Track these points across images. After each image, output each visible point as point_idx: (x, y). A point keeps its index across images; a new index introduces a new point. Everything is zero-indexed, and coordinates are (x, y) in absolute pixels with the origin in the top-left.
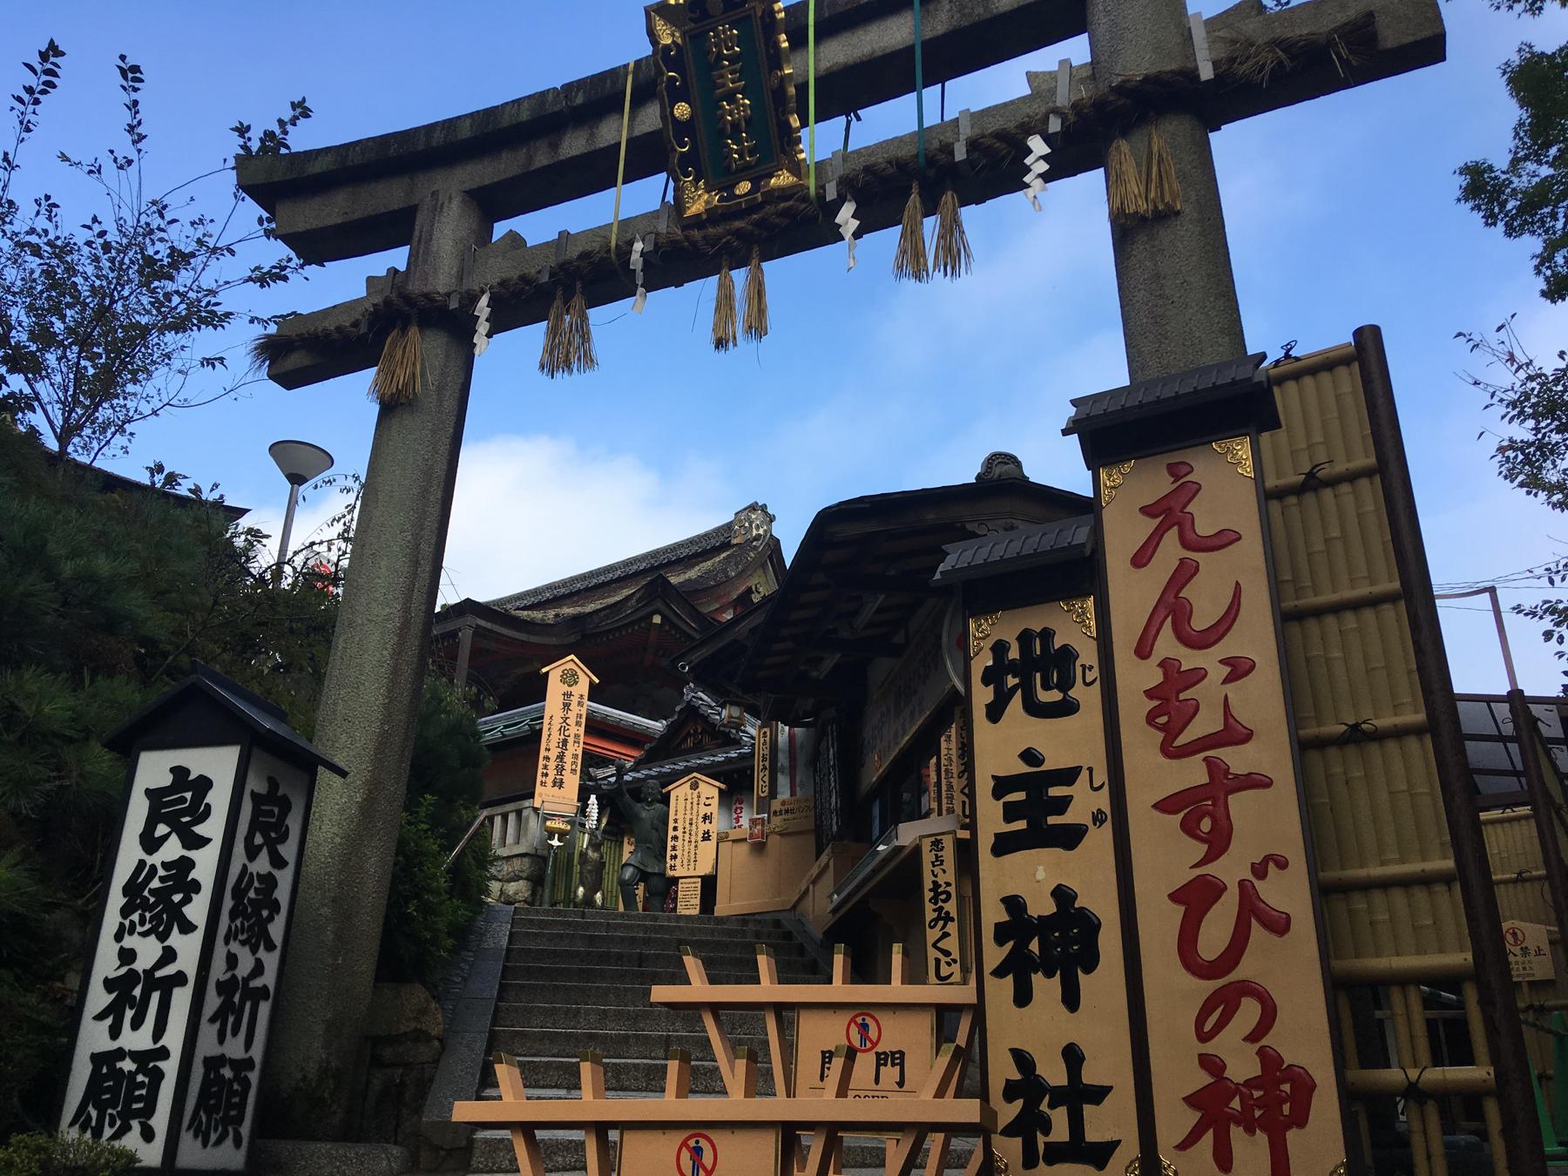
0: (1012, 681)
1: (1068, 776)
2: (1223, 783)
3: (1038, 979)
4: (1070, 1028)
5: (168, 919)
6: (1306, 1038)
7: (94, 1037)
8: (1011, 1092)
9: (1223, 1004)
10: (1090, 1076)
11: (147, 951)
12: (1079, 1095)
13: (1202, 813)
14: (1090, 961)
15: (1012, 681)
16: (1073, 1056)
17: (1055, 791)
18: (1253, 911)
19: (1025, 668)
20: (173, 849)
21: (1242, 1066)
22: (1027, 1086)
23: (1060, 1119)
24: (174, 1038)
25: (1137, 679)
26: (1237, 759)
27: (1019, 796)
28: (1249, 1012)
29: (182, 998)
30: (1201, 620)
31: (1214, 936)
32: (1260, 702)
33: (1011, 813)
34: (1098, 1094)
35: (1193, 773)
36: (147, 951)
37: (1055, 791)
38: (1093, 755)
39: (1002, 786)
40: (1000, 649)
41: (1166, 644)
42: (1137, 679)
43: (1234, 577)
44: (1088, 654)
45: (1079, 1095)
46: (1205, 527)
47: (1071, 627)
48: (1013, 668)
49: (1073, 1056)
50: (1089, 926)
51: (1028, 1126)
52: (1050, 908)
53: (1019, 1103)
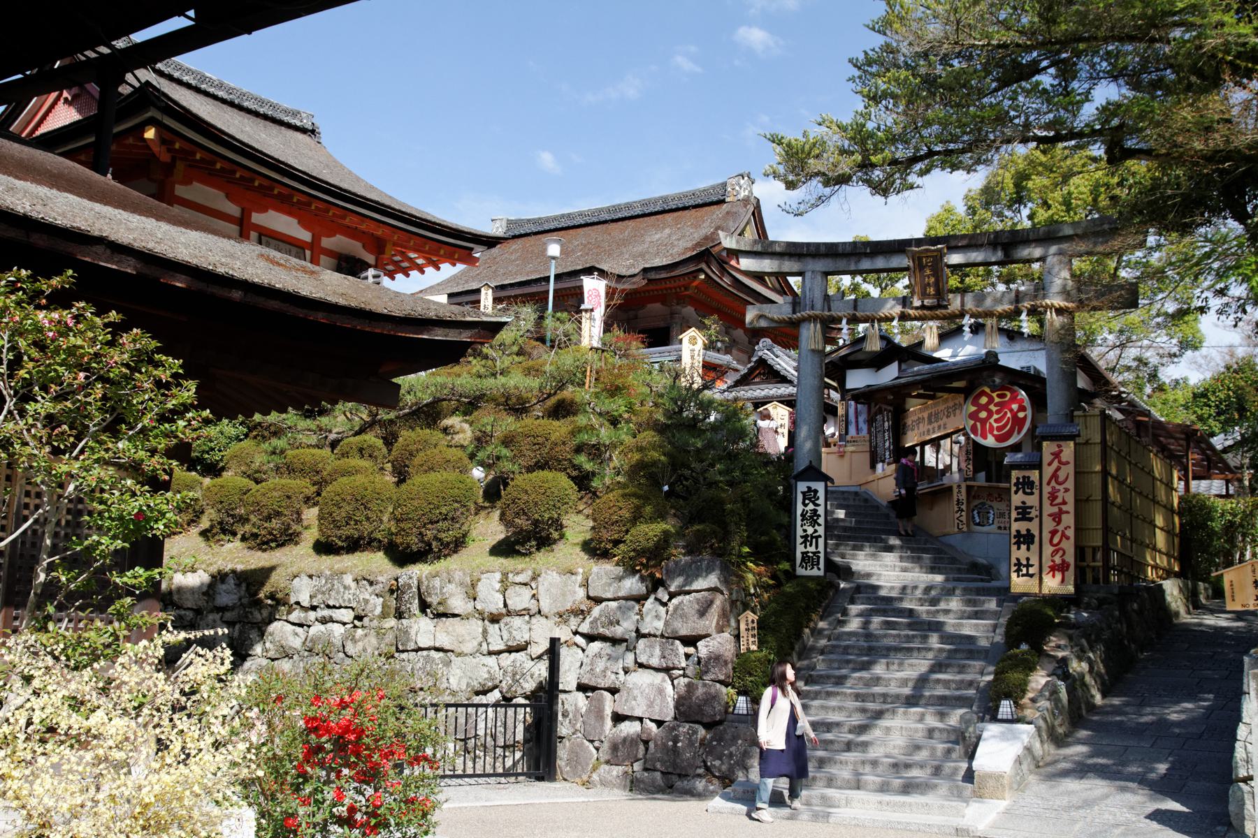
1: (1031, 507)
2: (1061, 512)
4: (1027, 554)
5: (814, 523)
6: (1070, 558)
7: (800, 549)
9: (1056, 552)
11: (810, 530)
12: (1028, 566)
13: (1057, 518)
14: (1033, 542)
16: (1028, 559)
18: (1063, 535)
19: (1023, 484)
20: (811, 506)
21: (1058, 560)
22: (1019, 564)
24: (821, 548)
25: (1047, 490)
26: (1064, 508)
28: (1061, 553)
29: (821, 541)
30: (1061, 479)
31: (1056, 541)
32: (1070, 498)
35: (1055, 509)
36: (810, 530)
38: (1037, 504)
39: (1017, 508)
40: (1018, 479)
41: (1053, 484)
42: (1047, 490)
43: (1069, 470)
44: (1037, 483)
46: (1064, 460)
47: (1034, 475)
49: (1028, 559)
50: (1033, 536)
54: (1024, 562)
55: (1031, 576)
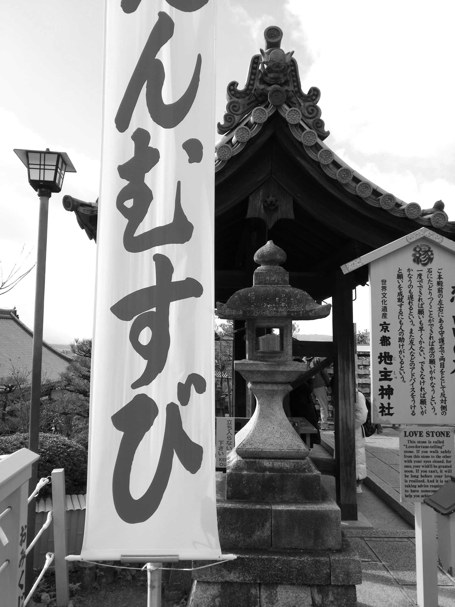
0: (383, 359)
1: (391, 372)
3: (385, 396)
8: (380, 408)
10: (391, 406)
12: (389, 408)
15: (383, 359)
16: (389, 404)
17: (388, 374)
23: (387, 411)
27: (383, 374)
33: (382, 376)
34: (392, 408)
37: (388, 374)
45: (389, 408)
48: (383, 357)
49: (389, 404)
51: (382, 412)
52: (387, 387)
54: (386, 406)
55: (391, 415)
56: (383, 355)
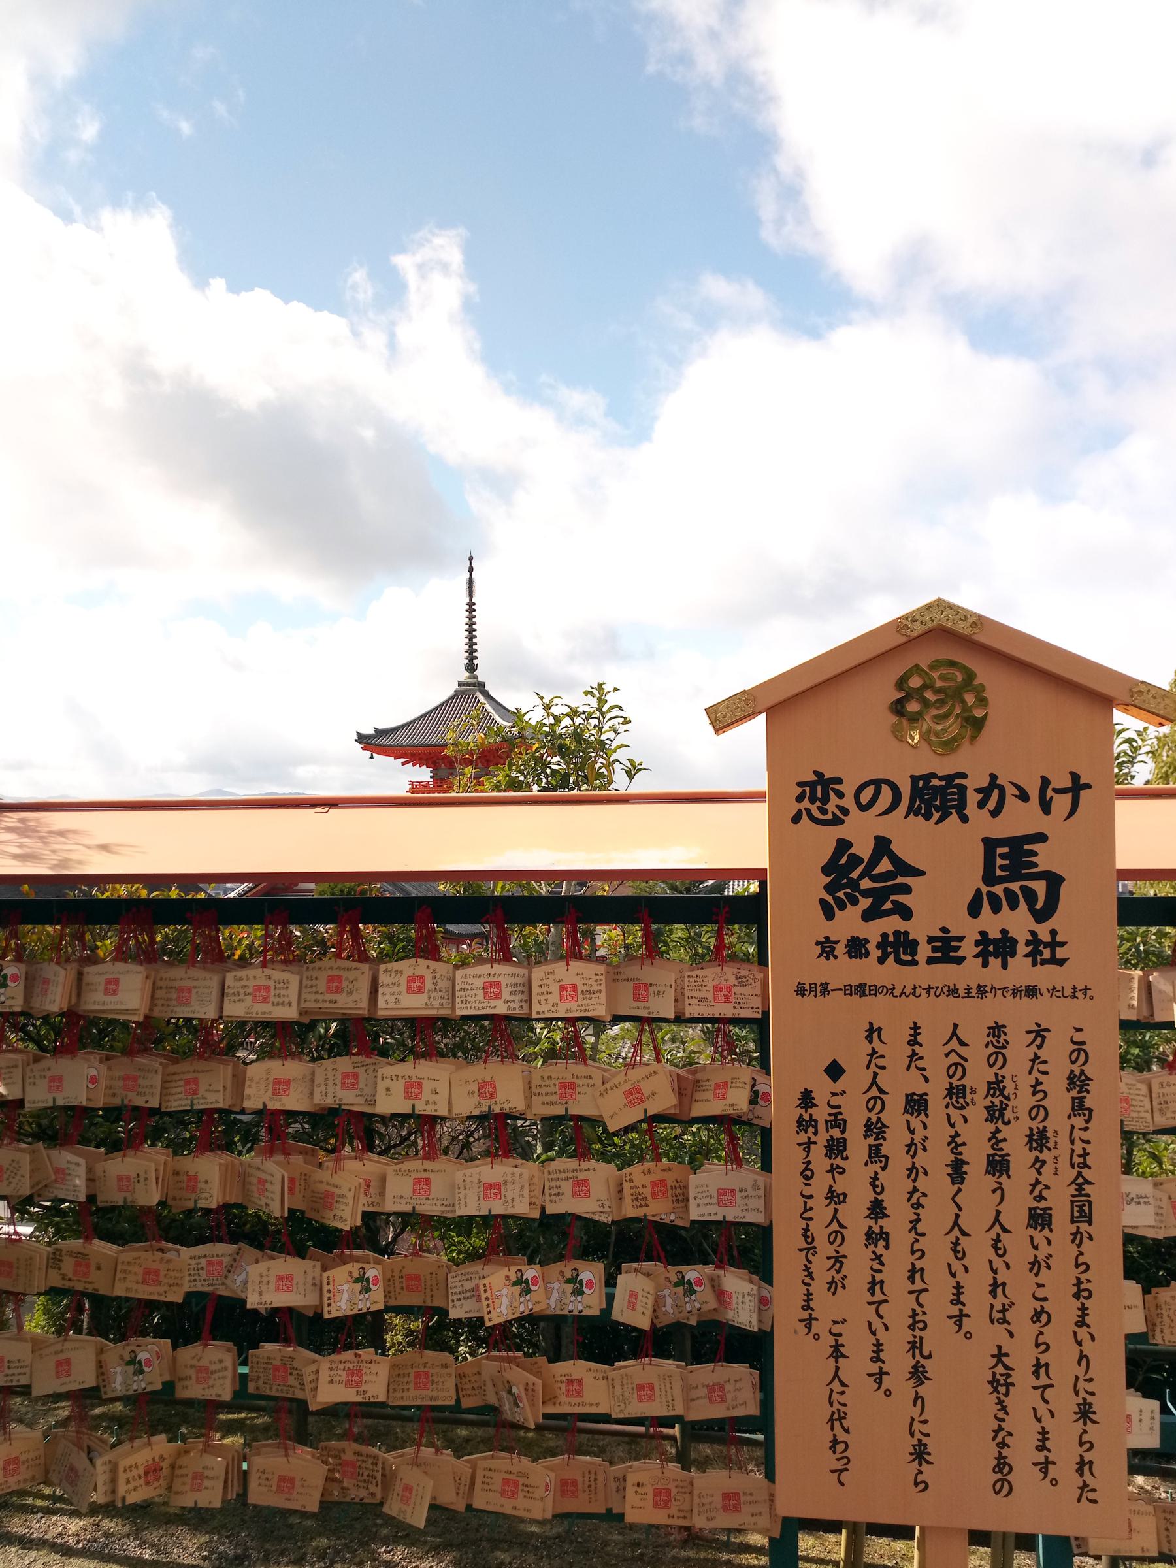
8: (1028, 943)
14: (1013, 954)
19: (896, 945)
23: (1047, 953)
27: (940, 944)
48: (891, 944)
53: (1031, 948)
56: (891, 939)
